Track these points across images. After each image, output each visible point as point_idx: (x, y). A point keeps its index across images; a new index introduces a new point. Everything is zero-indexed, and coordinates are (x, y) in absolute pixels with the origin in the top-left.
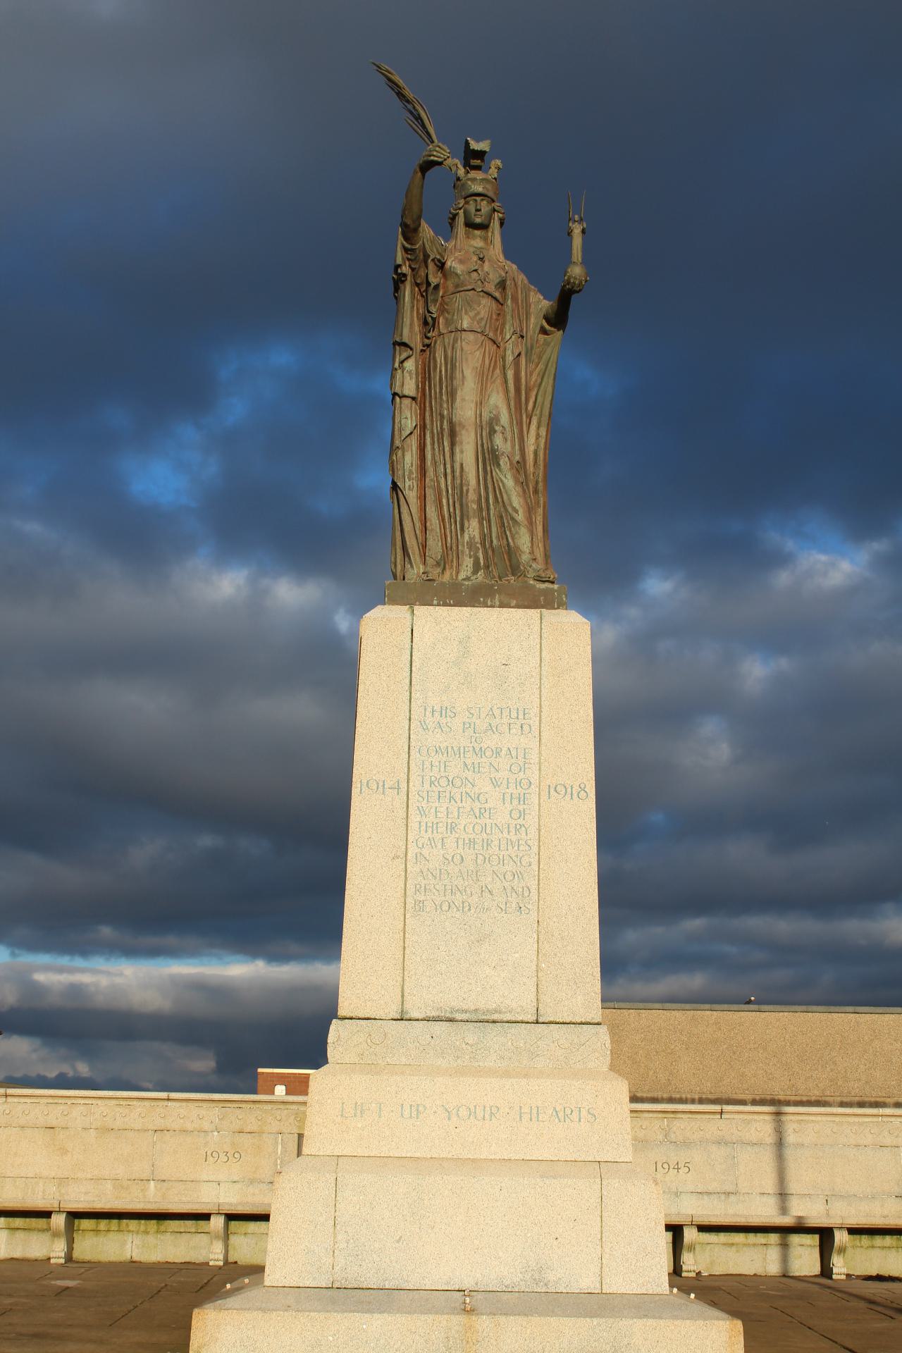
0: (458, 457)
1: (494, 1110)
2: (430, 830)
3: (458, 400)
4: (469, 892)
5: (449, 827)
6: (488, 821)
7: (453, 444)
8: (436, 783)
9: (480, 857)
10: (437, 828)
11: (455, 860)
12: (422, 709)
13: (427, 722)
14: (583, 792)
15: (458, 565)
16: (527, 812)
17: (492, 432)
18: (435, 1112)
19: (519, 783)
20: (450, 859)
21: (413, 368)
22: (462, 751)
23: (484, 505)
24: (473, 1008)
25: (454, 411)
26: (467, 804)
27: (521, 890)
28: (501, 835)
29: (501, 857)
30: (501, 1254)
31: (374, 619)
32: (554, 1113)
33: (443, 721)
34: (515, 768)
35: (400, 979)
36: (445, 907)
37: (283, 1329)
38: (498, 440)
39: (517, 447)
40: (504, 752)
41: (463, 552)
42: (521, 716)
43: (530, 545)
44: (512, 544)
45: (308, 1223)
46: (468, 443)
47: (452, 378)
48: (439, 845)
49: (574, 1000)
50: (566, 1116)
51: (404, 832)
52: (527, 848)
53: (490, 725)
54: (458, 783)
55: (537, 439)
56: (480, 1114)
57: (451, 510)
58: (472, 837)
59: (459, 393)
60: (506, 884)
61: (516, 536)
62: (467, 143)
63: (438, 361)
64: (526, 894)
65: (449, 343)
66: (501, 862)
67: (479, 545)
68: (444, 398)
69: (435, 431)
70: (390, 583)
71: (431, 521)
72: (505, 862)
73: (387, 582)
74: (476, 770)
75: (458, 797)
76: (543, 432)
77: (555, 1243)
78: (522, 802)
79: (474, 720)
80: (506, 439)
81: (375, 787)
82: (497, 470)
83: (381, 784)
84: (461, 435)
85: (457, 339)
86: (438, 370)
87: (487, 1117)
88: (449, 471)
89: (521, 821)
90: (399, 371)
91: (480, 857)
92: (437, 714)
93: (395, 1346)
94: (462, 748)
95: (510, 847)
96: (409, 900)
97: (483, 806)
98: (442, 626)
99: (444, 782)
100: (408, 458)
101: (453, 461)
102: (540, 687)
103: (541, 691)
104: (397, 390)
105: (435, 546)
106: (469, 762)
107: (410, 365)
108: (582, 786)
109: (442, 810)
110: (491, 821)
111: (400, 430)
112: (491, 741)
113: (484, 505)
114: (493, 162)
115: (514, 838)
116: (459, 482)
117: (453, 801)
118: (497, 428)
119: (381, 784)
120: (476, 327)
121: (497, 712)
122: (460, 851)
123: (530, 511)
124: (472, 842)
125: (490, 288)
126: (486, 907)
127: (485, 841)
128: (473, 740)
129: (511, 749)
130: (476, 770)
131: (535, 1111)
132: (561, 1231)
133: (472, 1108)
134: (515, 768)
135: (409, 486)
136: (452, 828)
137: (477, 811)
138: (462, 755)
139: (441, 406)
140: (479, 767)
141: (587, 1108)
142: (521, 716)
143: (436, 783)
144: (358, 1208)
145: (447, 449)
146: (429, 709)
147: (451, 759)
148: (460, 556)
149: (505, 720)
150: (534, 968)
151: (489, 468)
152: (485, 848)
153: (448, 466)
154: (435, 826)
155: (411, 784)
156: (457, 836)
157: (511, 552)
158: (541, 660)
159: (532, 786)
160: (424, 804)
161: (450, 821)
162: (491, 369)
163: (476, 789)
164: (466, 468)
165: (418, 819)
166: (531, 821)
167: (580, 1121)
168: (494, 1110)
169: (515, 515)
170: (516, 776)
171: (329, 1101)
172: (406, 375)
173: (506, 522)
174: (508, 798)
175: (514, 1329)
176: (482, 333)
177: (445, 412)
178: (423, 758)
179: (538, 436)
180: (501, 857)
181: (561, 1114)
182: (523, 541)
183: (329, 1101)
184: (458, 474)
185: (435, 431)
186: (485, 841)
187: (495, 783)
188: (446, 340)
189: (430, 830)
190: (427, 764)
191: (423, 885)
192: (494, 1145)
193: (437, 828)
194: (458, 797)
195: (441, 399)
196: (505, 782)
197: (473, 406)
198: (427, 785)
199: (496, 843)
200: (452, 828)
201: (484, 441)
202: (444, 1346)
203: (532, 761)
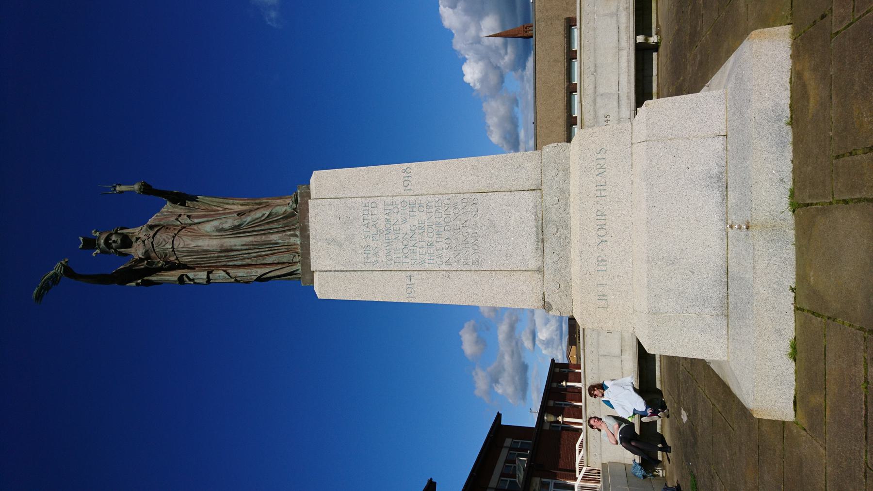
0: (239, 248)
1: (599, 213)
2: (433, 258)
3: (208, 248)
4: (467, 234)
5: (430, 247)
6: (426, 224)
7: (232, 250)
8: (407, 255)
9: (446, 228)
10: (431, 253)
11: (449, 243)
12: (367, 264)
13: (373, 261)
14: (407, 171)
15: (294, 245)
16: (419, 202)
17: (222, 230)
18: (602, 250)
20: (448, 245)
21: (193, 273)
22: (388, 241)
23: (262, 232)
24: (535, 229)
25: (215, 250)
26: (417, 237)
27: (464, 204)
28: (433, 217)
29: (445, 216)
30: (700, 205)
31: (320, 292)
32: (600, 175)
34: (396, 210)
35: (519, 273)
36: (476, 247)
37: (768, 355)
38: (226, 226)
39: (230, 216)
41: (288, 243)
42: (367, 208)
43: (282, 207)
44: (281, 216)
45: (682, 332)
46: (230, 242)
47: (197, 252)
48: (441, 252)
49: (528, 168)
50: (601, 168)
51: (435, 272)
52: (440, 201)
54: (405, 242)
55: (235, 205)
56: (603, 222)
57: (267, 249)
59: (205, 248)
60: (461, 212)
61: (277, 214)
62: (81, 248)
63: (190, 260)
64: (466, 201)
65: (181, 255)
67: (284, 234)
68: (209, 256)
69: (227, 260)
70: (303, 283)
71: (274, 261)
72: (448, 214)
73: (303, 285)
74: (398, 232)
75: (413, 242)
76: (231, 201)
77: (691, 169)
78: (415, 206)
79: (370, 235)
80: (226, 222)
81: (411, 289)
82: (242, 226)
83: (408, 286)
84: (226, 246)
85: (178, 250)
86: (195, 260)
87: (604, 217)
88: (247, 252)
89: (425, 206)
90: (195, 281)
92: (369, 256)
93: (779, 277)
94: (387, 241)
95: (440, 211)
96: (473, 268)
97: (418, 228)
98: (320, 254)
99: (406, 251)
100: (240, 274)
101: (242, 250)
102: (351, 198)
103: (353, 197)
104: (204, 281)
105: (286, 257)
106: (394, 237)
107: (191, 275)
108: (404, 171)
111: (225, 279)
112: (382, 225)
113: (262, 232)
114: (93, 234)
115: (435, 209)
116: (251, 247)
117: (416, 245)
118: (221, 227)
119: (408, 286)
120: (171, 241)
121: (366, 222)
122: (443, 240)
123: (267, 205)
124: (438, 233)
125: (152, 233)
127: (437, 226)
128: (382, 235)
130: (398, 232)
132: (682, 165)
133: (598, 227)
134: (396, 210)
135: (255, 273)
139: (213, 257)
140: (396, 231)
141: (596, 155)
142: (367, 208)
143: (407, 255)
144: (670, 299)
145: (235, 253)
146: (366, 260)
147: (393, 247)
148: (290, 244)
150: (509, 193)
151: (242, 231)
152: (441, 225)
153: (244, 252)
155: (408, 269)
156: (435, 242)
157: (287, 216)
158: (336, 198)
159: (405, 200)
161: (427, 247)
162: (194, 231)
164: (244, 243)
165: (427, 264)
166: (424, 200)
167: (604, 159)
168: (599, 213)
169: (266, 216)
170: (400, 209)
171: (598, 316)
172: (197, 277)
173: (270, 219)
174: (412, 214)
175: (764, 194)
176: (174, 237)
177: (216, 255)
178: (393, 263)
179: (233, 204)
181: (601, 171)
182: (281, 210)
184: (247, 247)
185: (227, 260)
186: (437, 226)
187: (405, 221)
188: (180, 256)
189: (433, 258)
190: (396, 260)
192: (623, 212)
193: (431, 253)
194: (413, 242)
195: (210, 257)
196: (404, 216)
197: (211, 240)
198: (408, 260)
199: (437, 219)
201: (228, 233)
202: (778, 242)
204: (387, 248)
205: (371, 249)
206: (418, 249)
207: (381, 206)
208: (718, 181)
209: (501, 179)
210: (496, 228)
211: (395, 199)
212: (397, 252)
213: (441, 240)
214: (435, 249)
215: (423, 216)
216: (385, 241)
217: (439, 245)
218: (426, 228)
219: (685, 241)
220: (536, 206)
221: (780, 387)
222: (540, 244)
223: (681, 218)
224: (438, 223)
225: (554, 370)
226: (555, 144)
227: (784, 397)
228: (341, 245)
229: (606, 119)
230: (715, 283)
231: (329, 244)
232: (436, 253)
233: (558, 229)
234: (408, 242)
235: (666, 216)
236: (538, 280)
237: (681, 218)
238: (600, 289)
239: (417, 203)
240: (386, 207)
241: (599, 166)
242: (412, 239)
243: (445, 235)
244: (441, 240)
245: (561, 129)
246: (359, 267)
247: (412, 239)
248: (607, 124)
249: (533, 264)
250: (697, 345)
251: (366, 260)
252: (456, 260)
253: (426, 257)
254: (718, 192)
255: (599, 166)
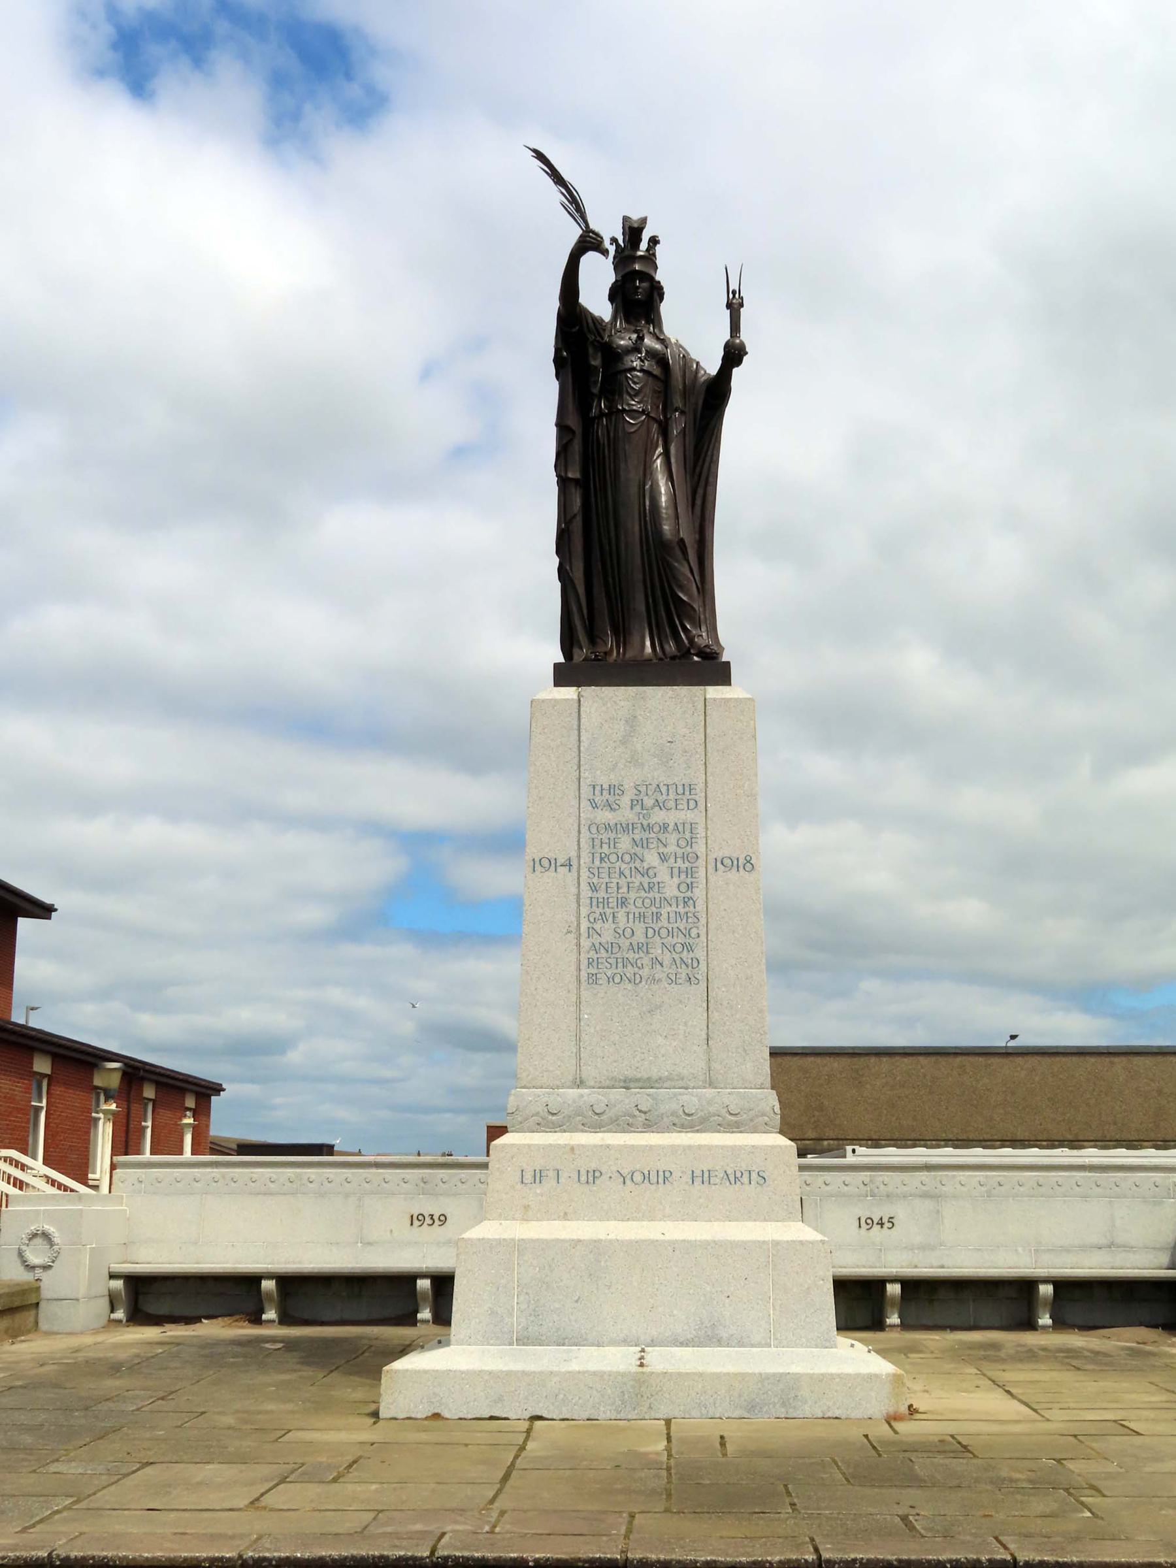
1: (667, 1174)
2: (601, 905)
4: (640, 965)
5: (620, 901)
6: (657, 896)
8: (606, 860)
9: (650, 931)
10: (608, 903)
13: (596, 800)
18: (611, 1177)
19: (684, 857)
20: (621, 932)
22: (630, 827)
24: (646, 1076)
26: (637, 880)
27: (690, 961)
29: (670, 929)
32: (726, 1177)
33: (611, 799)
36: (617, 980)
40: (671, 828)
42: (687, 793)
48: (611, 919)
52: (696, 920)
53: (657, 801)
56: (654, 1179)
58: (643, 910)
60: (676, 957)
64: (695, 965)
66: (671, 933)
77: (727, 1301)
78: (689, 876)
83: (553, 862)
87: (661, 1180)
89: (689, 894)
91: (650, 931)
92: (605, 792)
93: (574, 1401)
94: (630, 825)
95: (679, 920)
96: (584, 974)
97: (652, 881)
98: (609, 705)
99: (613, 858)
102: (705, 763)
106: (637, 837)
109: (612, 885)
110: (660, 895)
112: (658, 816)
117: (623, 877)
119: (553, 862)
121: (664, 789)
126: (657, 979)
127: (655, 914)
128: (641, 817)
129: (678, 825)
130: (645, 845)
131: (706, 1175)
134: (683, 843)
136: (623, 903)
137: (646, 886)
138: (631, 832)
140: (647, 843)
141: (757, 1170)
142: (687, 793)
143: (606, 860)
146: (598, 788)
147: (619, 836)
149: (672, 796)
150: (705, 1036)
152: (655, 921)
154: (606, 901)
156: (627, 910)
160: (595, 880)
161: (620, 896)
163: (646, 865)
165: (590, 895)
166: (699, 893)
168: (667, 1174)
170: (683, 850)
171: (509, 1169)
174: (676, 871)
175: (686, 1384)
178: (593, 836)
180: (670, 929)
183: (509, 1169)
186: (655, 914)
187: (663, 858)
189: (601, 905)
190: (597, 842)
191: (595, 959)
193: (608, 903)
194: (627, 873)
198: (597, 862)
199: (665, 916)
200: (623, 902)
203: (698, 836)
204: (619, 826)
205: (618, 797)
206: (615, 881)
207: (690, 816)
208: (708, 1336)
209: (728, 1023)
210: (649, 1015)
211: (702, 842)
212: (612, 843)
213: (631, 920)
214: (616, 910)
215: (671, 891)
216: (630, 822)
217: (621, 915)
218: (651, 895)
219: (623, 1292)
220: (682, 1079)
221: (425, 1400)
222: (622, 1084)
223: (656, 1286)
224: (658, 916)
225: (191, 1091)
226: (777, 1110)
227: (412, 1405)
228: (624, 742)
229: (885, 1220)
230: (562, 1329)
231: (626, 721)
232: (608, 911)
233: (645, 1113)
234: (628, 863)
235: (660, 1266)
236: (563, 1081)
237: (656, 1286)
238: (552, 1174)
239: (693, 880)
240: (688, 827)
241: (738, 1175)
242: (633, 869)
243: (639, 929)
244: (631, 920)
245: (955, 1130)
246: (587, 774)
247: (633, 869)
248: (875, 1222)
249: (589, 1072)
250: (473, 1305)
251: (598, 788)
252: (597, 945)
253: (602, 894)
254: (692, 1336)
255: (738, 1175)
